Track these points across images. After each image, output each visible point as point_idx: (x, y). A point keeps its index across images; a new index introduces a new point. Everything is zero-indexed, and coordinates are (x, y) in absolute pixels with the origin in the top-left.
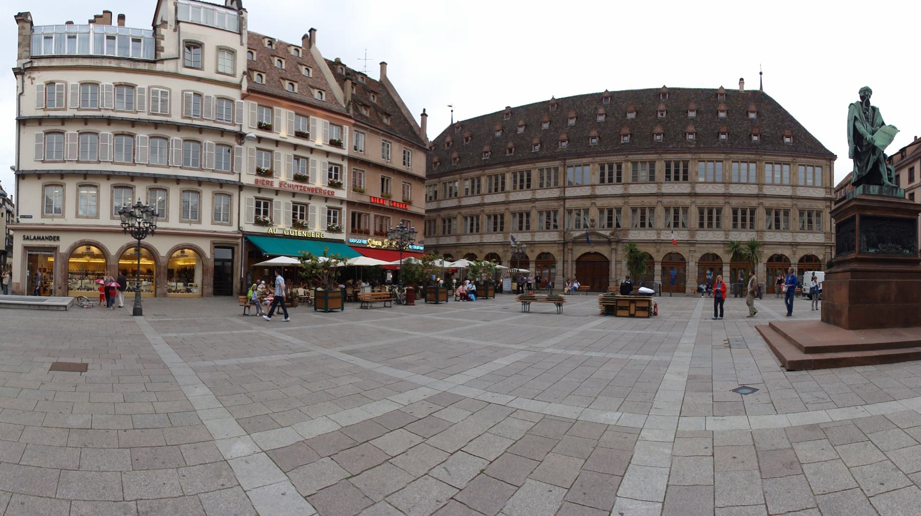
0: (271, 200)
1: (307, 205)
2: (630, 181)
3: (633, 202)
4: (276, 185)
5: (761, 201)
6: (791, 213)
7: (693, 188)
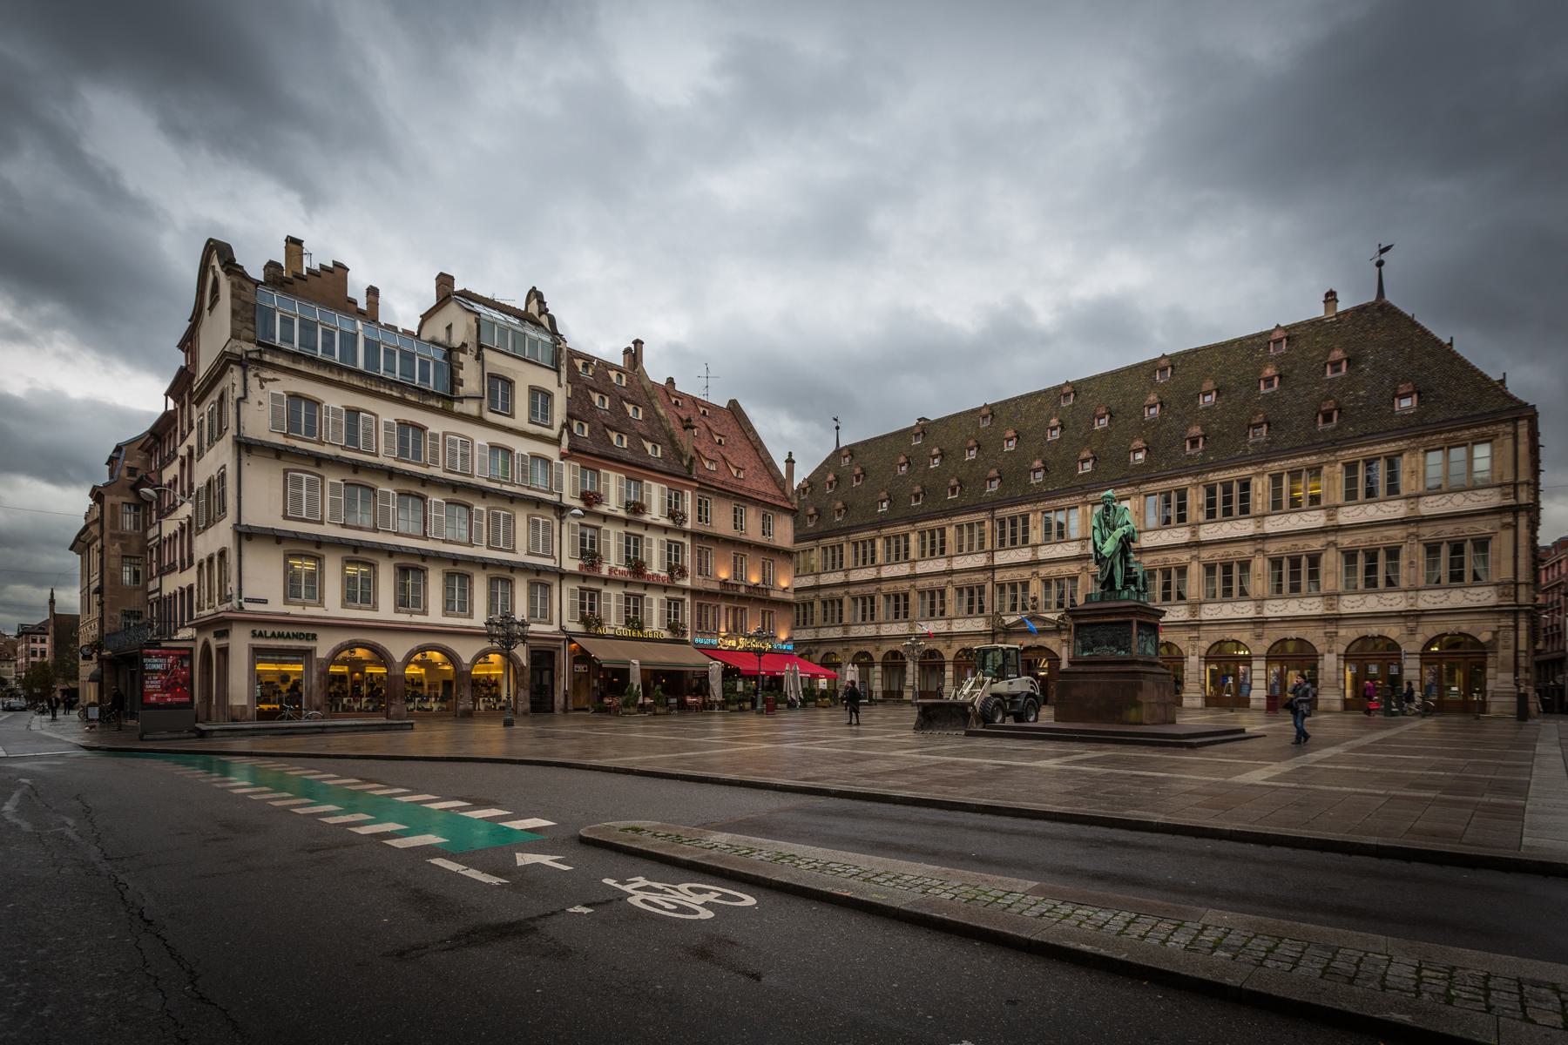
0: (599, 591)
1: (642, 596)
4: (605, 572)
6: (1403, 554)
7: (1194, 533)
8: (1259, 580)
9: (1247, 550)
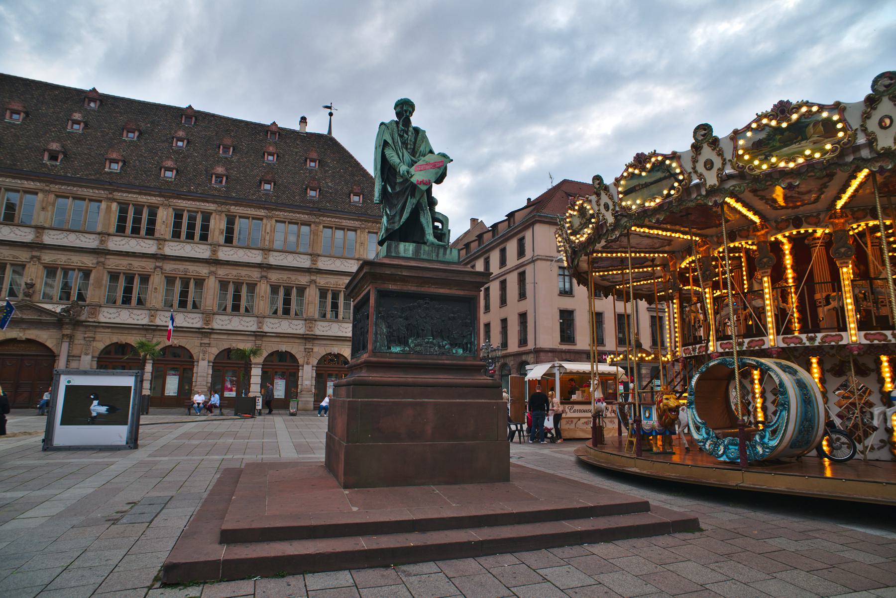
2: (113, 230)
3: (113, 263)
5: (313, 278)
7: (214, 252)
8: (263, 300)
9: (255, 274)
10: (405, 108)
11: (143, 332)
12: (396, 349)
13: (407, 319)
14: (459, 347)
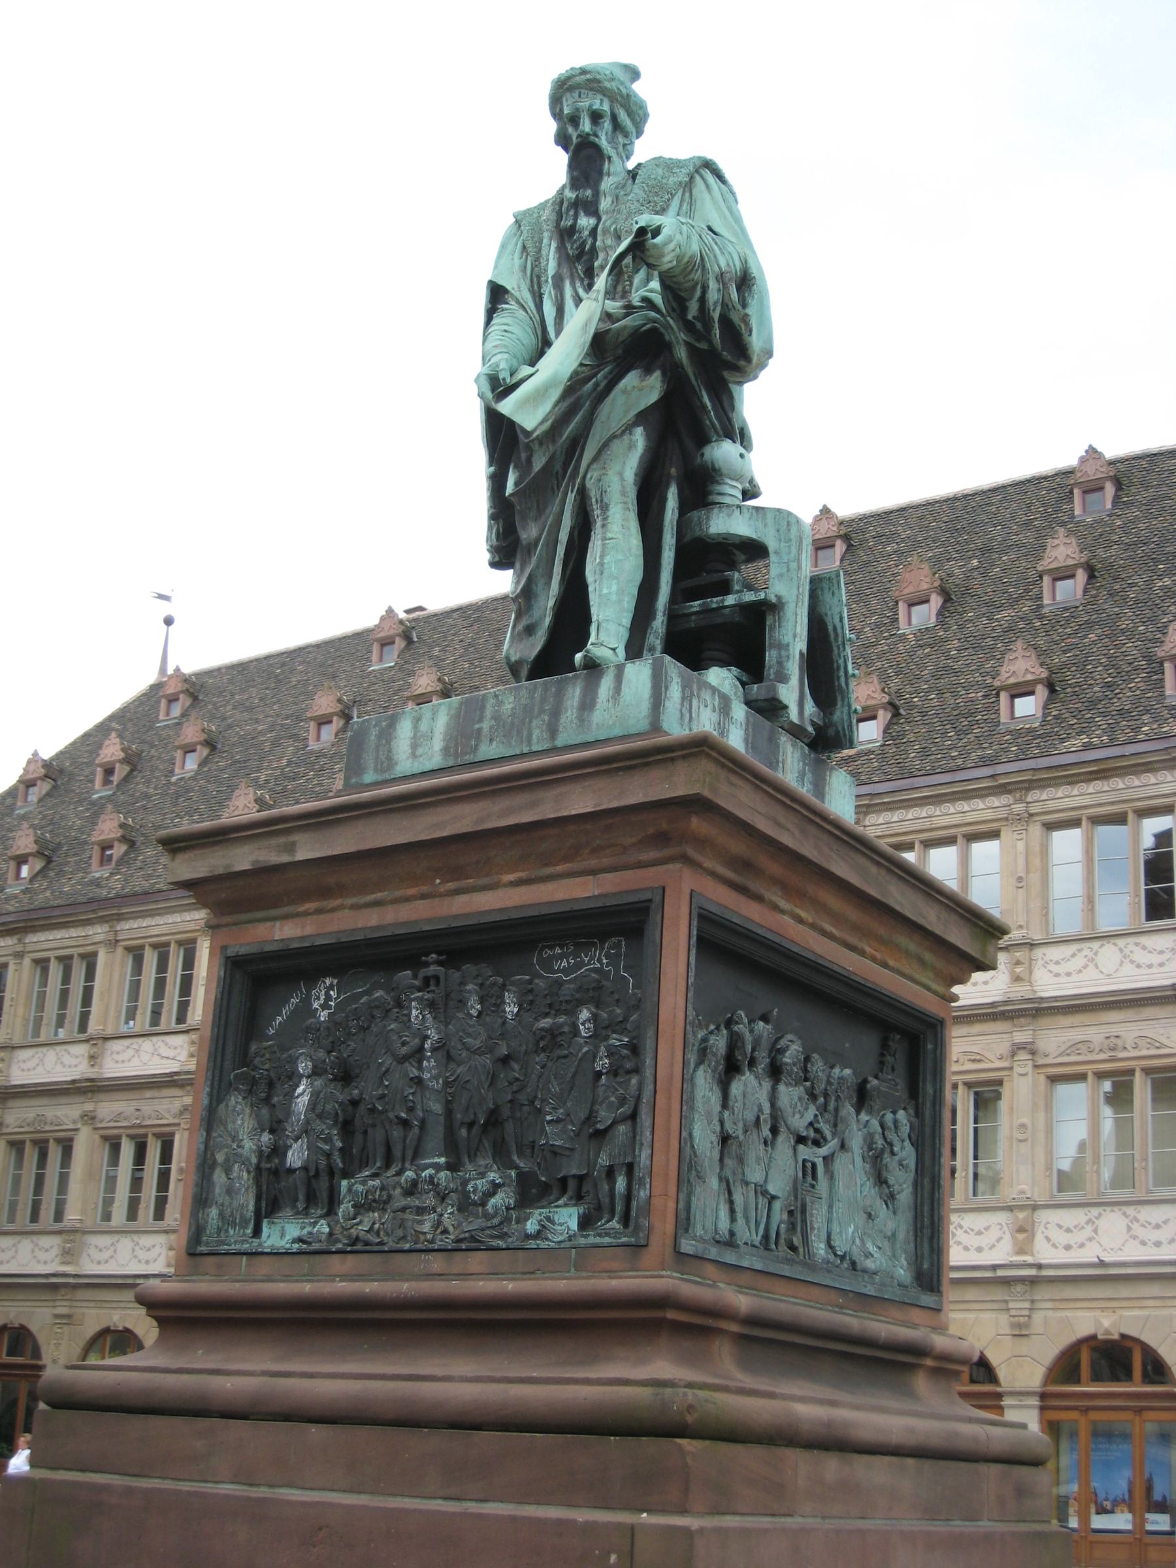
10: (593, 116)
11: (999, 1294)
12: (282, 1233)
13: (345, 1076)
14: (579, 1198)
